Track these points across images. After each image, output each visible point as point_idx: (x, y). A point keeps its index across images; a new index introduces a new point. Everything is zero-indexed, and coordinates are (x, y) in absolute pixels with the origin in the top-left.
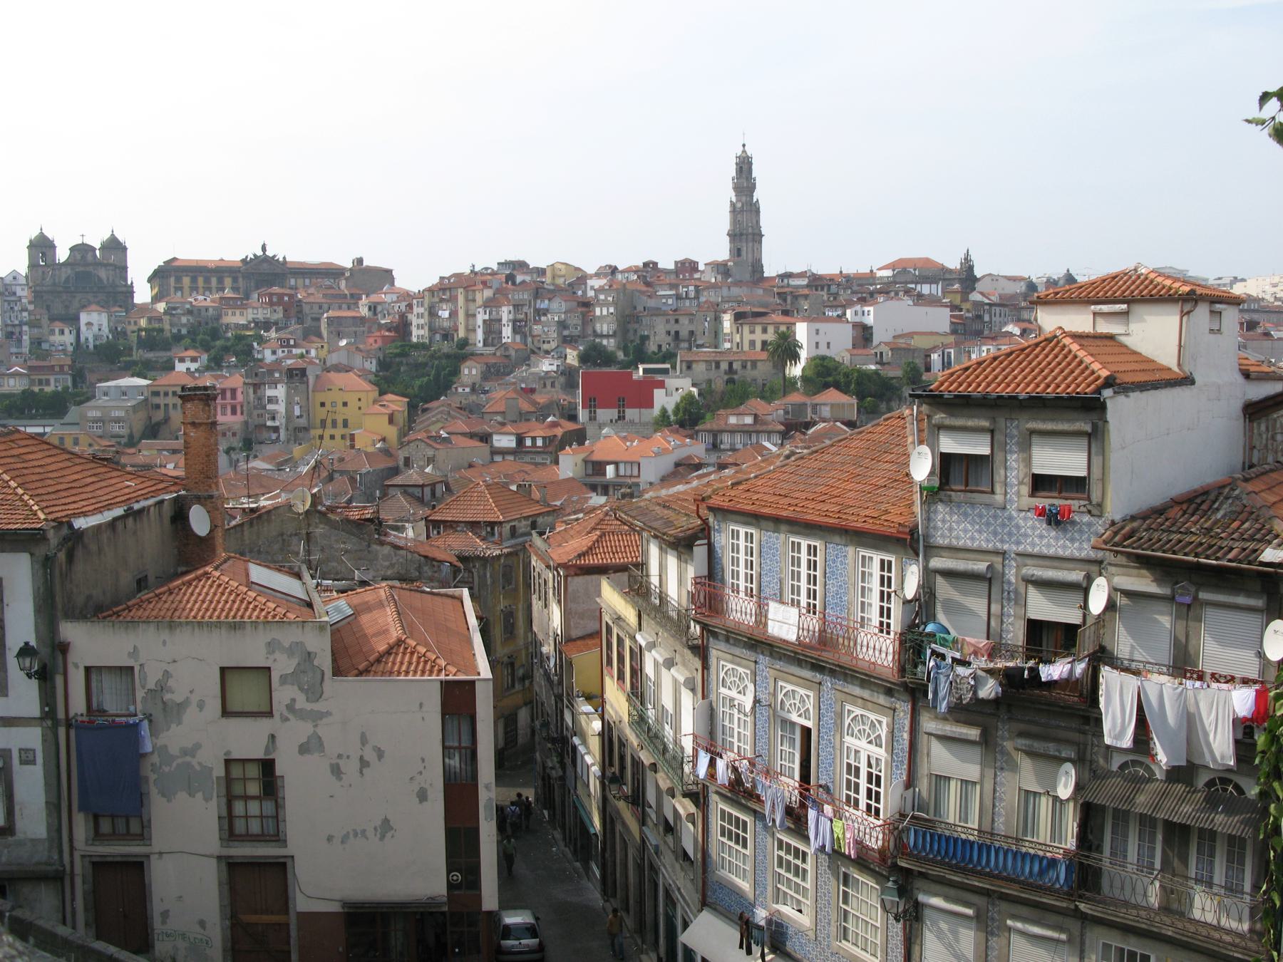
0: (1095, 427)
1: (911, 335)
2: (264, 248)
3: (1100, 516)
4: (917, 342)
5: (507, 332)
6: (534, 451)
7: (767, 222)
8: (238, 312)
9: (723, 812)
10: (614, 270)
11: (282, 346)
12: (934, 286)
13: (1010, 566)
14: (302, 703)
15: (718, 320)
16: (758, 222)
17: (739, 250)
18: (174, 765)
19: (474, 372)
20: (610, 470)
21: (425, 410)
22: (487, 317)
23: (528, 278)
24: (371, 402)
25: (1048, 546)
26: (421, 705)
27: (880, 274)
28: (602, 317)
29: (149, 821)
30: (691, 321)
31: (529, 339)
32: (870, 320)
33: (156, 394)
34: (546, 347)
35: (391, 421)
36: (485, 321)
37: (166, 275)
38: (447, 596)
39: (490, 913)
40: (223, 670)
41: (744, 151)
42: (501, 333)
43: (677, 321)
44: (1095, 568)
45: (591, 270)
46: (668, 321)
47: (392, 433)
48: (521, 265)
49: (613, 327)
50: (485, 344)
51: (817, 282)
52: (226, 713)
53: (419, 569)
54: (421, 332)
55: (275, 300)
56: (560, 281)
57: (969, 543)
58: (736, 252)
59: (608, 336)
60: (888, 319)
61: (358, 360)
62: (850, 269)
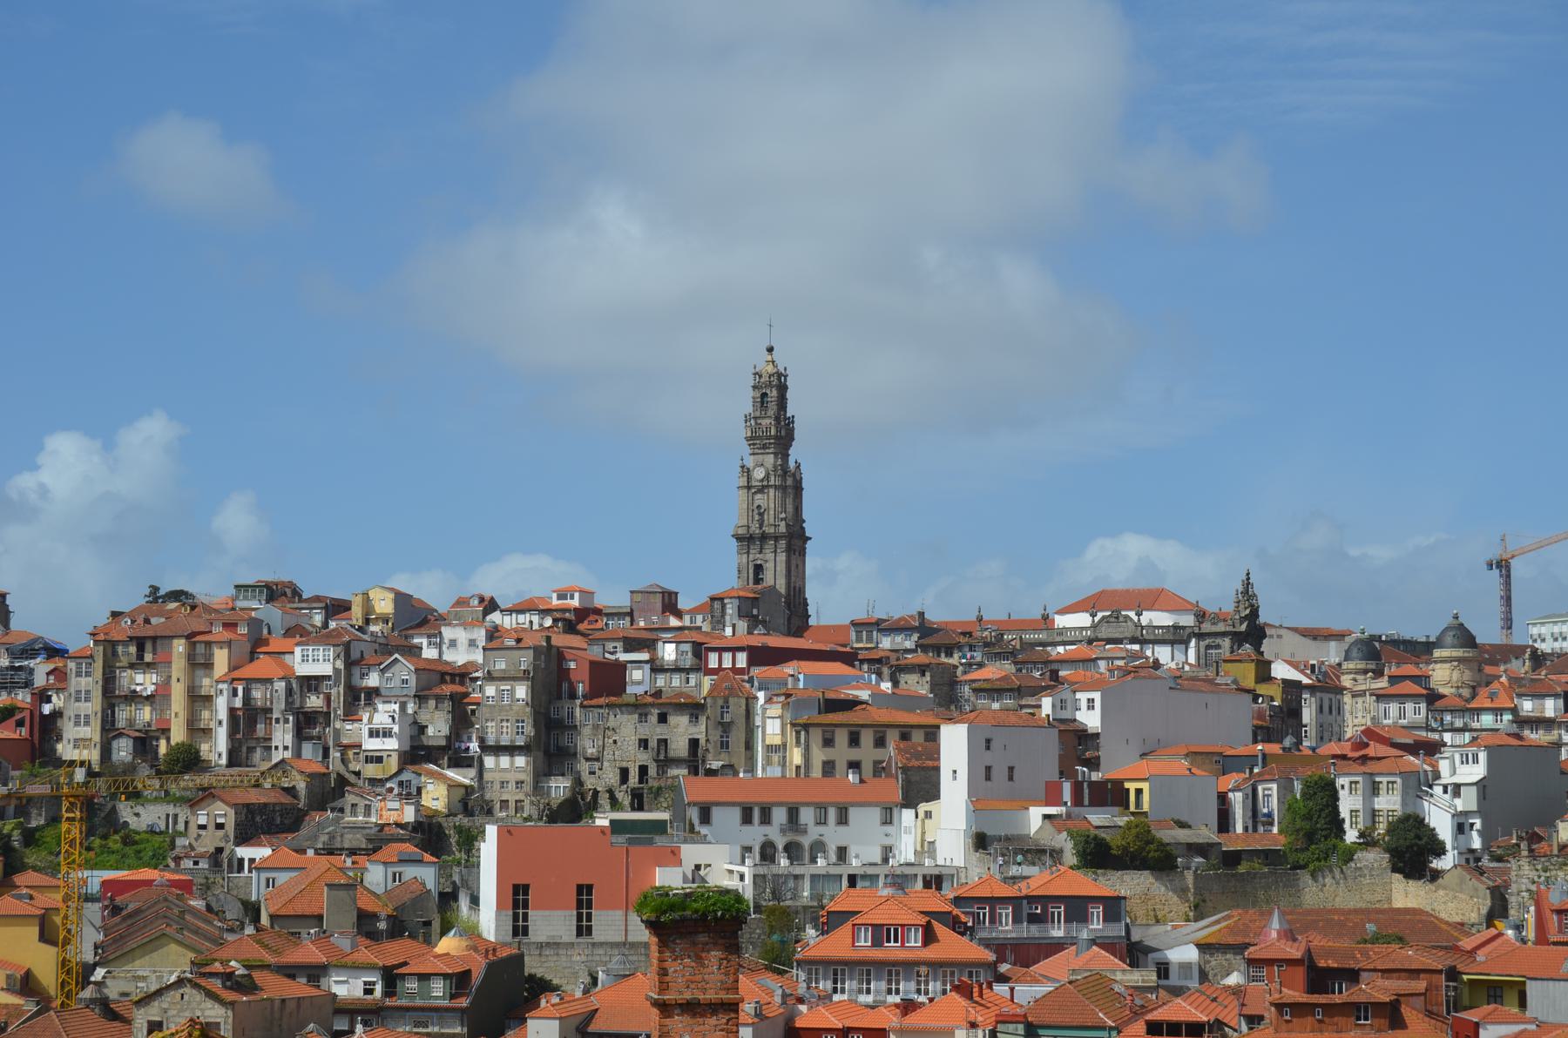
10: (491, 606)
12: (1179, 648)
16: (798, 509)
17: (759, 569)
27: (1062, 621)
30: (694, 718)
31: (335, 754)
32: (1091, 719)
34: (371, 770)
36: (232, 711)
43: (663, 719)
45: (441, 604)
46: (643, 717)
49: (529, 730)
50: (230, 764)
62: (994, 613)
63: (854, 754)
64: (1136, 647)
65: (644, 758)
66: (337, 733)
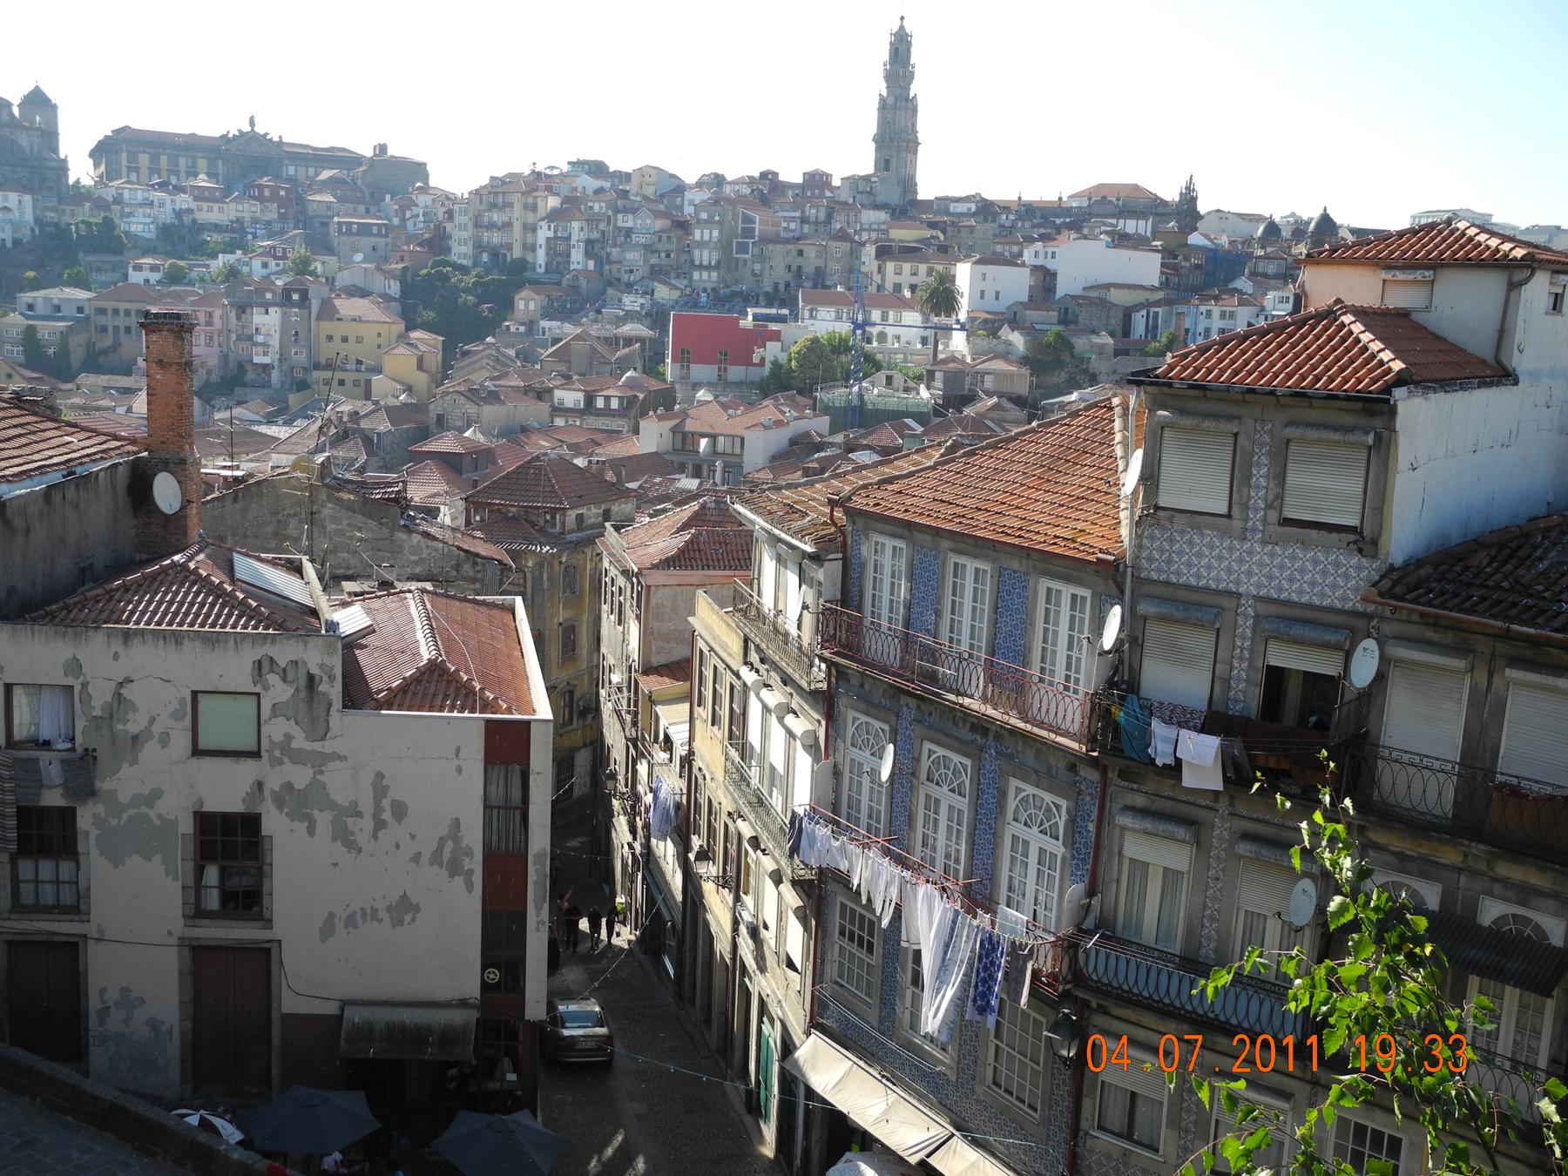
0: (1378, 438)
1: (1108, 286)
2: (252, 122)
3: (1375, 556)
4: (1116, 296)
5: (577, 257)
6: (607, 412)
7: (925, 127)
8: (216, 206)
9: (843, 906)
10: (718, 180)
11: (276, 258)
12: (1142, 223)
13: (1246, 616)
14: (300, 742)
15: (855, 253)
16: (914, 125)
18: (125, 817)
19: (532, 306)
20: (703, 442)
21: (465, 354)
22: (551, 234)
23: (607, 185)
24: (394, 337)
25: (1301, 592)
26: (458, 750)
28: (702, 244)
29: (88, 889)
32: (1051, 265)
33: (102, 311)
35: (420, 367)
36: (548, 239)
37: (117, 149)
38: (493, 605)
39: (538, 1025)
40: (195, 694)
41: (902, 27)
42: (569, 255)
43: (800, 253)
44: (1360, 624)
45: (690, 178)
46: (788, 252)
47: (421, 380)
48: (597, 169)
50: (547, 271)
51: (986, 209)
52: (197, 752)
53: (457, 567)
54: (464, 249)
55: (267, 193)
56: (649, 191)
57: (1193, 582)
58: (883, 164)
59: (709, 268)
60: (1082, 263)
61: (379, 283)
63: (914, 280)
64: (1114, 221)
65: (788, 277)
66: (608, 255)
